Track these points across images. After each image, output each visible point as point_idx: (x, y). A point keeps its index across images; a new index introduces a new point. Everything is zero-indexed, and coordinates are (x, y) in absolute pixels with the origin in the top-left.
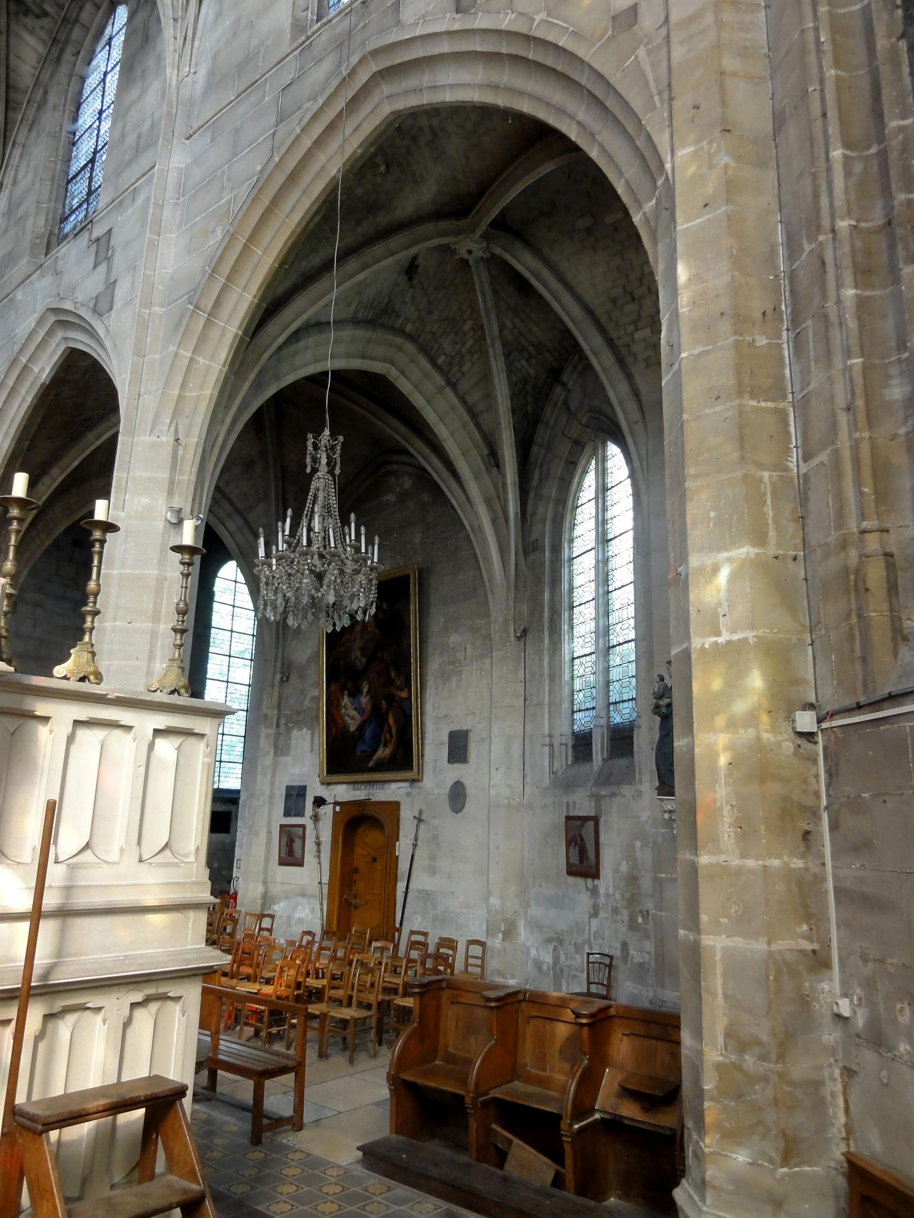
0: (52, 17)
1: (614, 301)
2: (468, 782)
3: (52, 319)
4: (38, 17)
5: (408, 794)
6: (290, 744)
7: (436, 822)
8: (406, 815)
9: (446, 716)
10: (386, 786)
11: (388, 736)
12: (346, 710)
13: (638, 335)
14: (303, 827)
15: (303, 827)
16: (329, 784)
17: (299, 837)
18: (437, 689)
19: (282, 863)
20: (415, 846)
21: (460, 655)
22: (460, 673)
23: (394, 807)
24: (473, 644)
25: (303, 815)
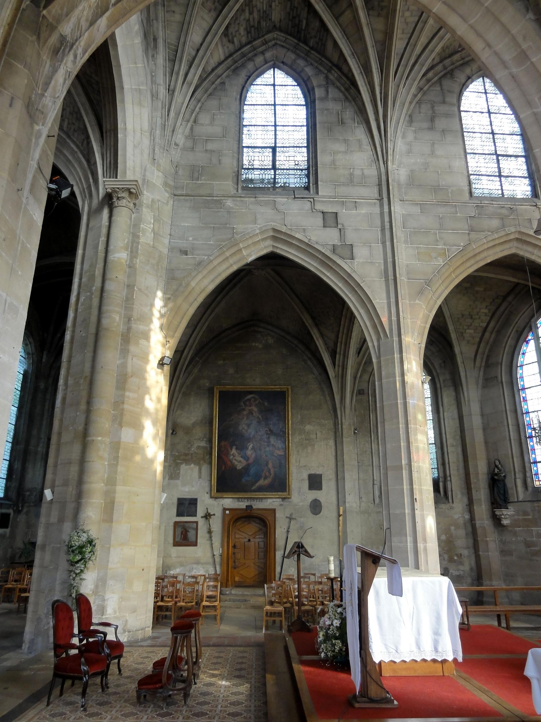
0: (235, 45)
1: (463, 316)
2: (322, 500)
3: (271, 234)
4: (229, 41)
5: (281, 505)
6: (179, 473)
7: (302, 519)
8: (279, 515)
9: (305, 466)
10: (264, 500)
11: (267, 474)
12: (234, 456)
13: (468, 331)
14: (197, 523)
15: (197, 523)
16: (216, 498)
17: (193, 529)
18: (298, 452)
19: (176, 544)
20: (288, 531)
21: (313, 436)
22: (314, 445)
23: (273, 511)
24: (321, 432)
25: (196, 516)
